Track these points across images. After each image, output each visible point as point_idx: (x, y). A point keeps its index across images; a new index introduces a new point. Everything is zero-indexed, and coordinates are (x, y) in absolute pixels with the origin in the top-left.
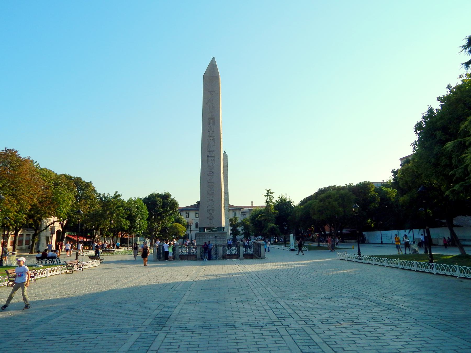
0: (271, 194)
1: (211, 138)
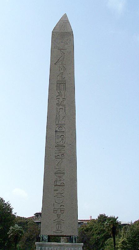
1: (61, 107)
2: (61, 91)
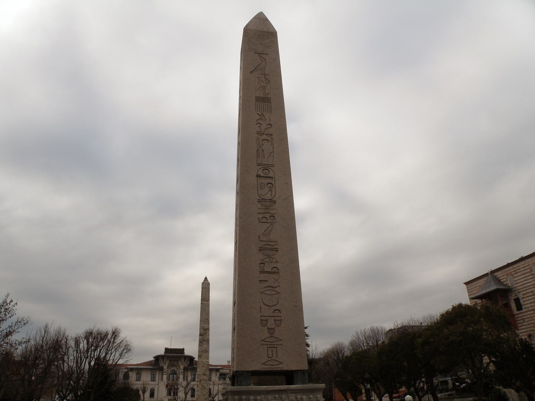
1: (264, 137)
2: (264, 114)
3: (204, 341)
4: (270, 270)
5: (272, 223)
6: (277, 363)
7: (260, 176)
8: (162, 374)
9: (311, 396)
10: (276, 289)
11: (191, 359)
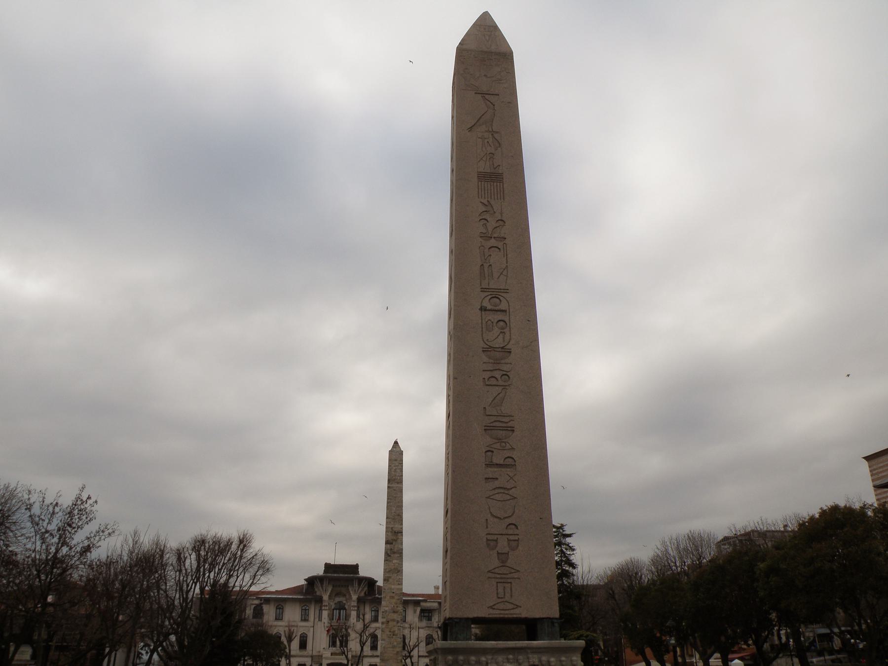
0: (568, 540)
1: (493, 242)
2: (492, 202)
3: (394, 553)
4: (502, 462)
5: (504, 387)
6: (511, 606)
7: (485, 310)
8: (321, 610)
9: (563, 659)
10: (511, 492)
11: (371, 582)
